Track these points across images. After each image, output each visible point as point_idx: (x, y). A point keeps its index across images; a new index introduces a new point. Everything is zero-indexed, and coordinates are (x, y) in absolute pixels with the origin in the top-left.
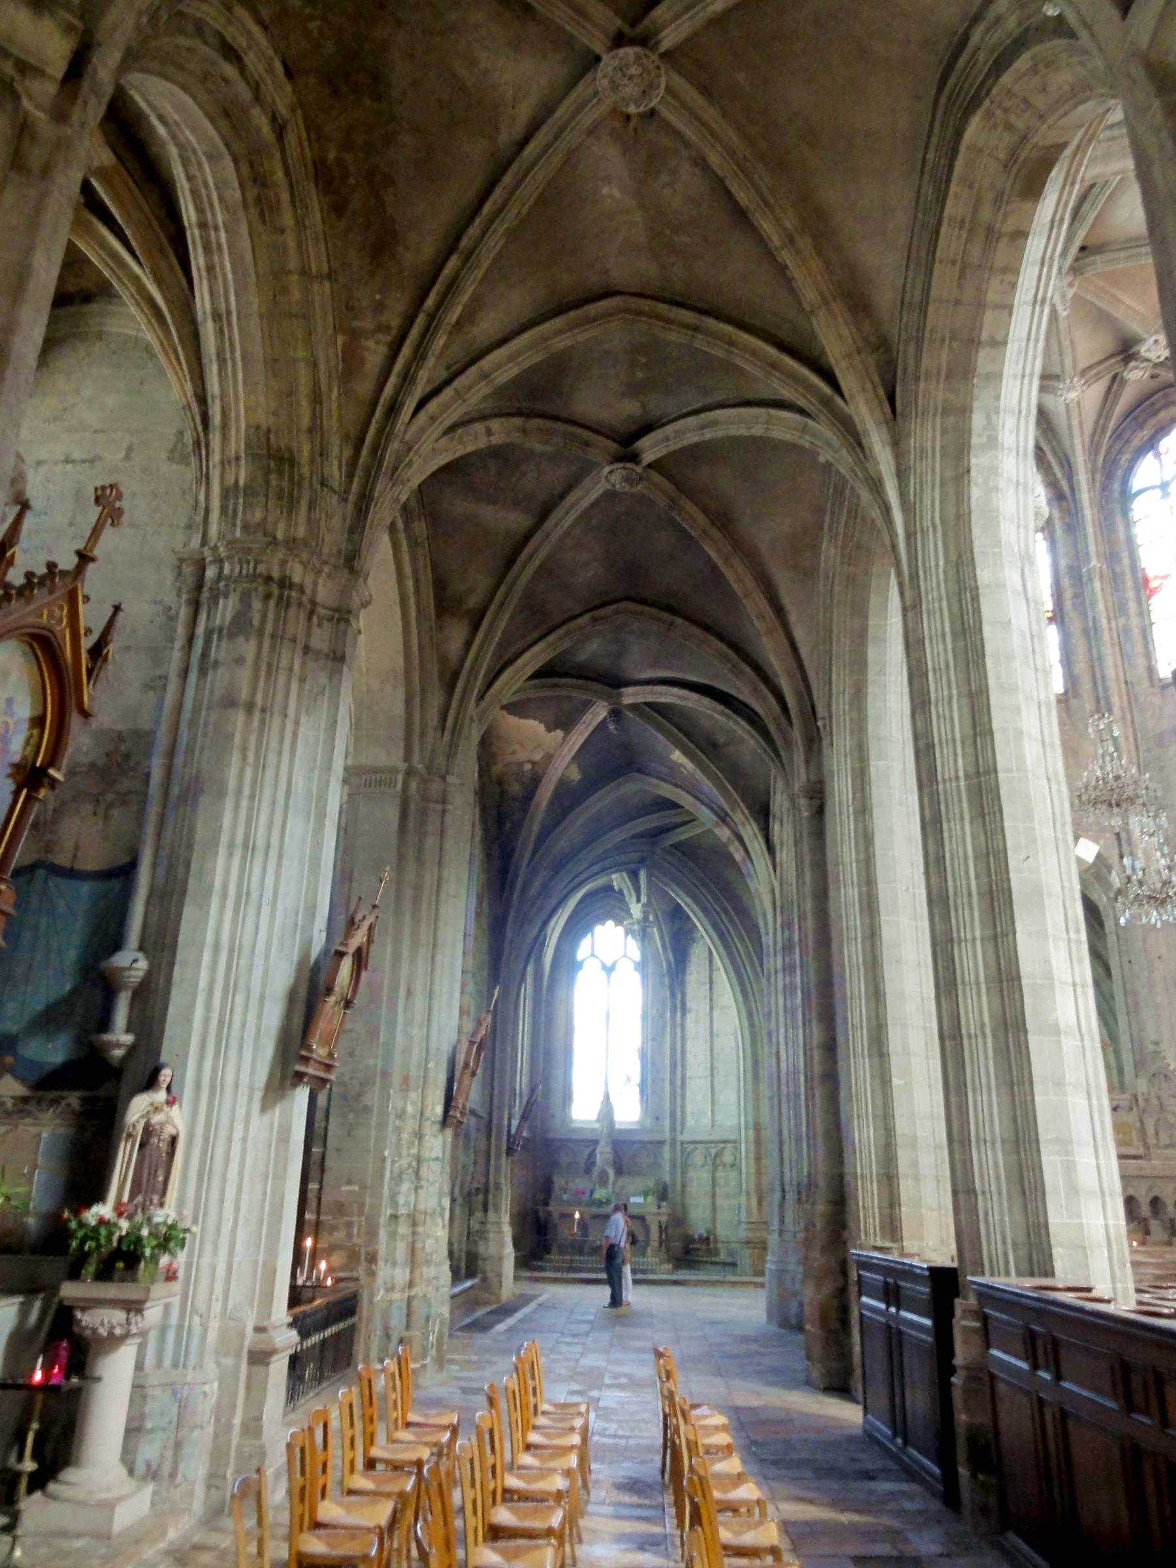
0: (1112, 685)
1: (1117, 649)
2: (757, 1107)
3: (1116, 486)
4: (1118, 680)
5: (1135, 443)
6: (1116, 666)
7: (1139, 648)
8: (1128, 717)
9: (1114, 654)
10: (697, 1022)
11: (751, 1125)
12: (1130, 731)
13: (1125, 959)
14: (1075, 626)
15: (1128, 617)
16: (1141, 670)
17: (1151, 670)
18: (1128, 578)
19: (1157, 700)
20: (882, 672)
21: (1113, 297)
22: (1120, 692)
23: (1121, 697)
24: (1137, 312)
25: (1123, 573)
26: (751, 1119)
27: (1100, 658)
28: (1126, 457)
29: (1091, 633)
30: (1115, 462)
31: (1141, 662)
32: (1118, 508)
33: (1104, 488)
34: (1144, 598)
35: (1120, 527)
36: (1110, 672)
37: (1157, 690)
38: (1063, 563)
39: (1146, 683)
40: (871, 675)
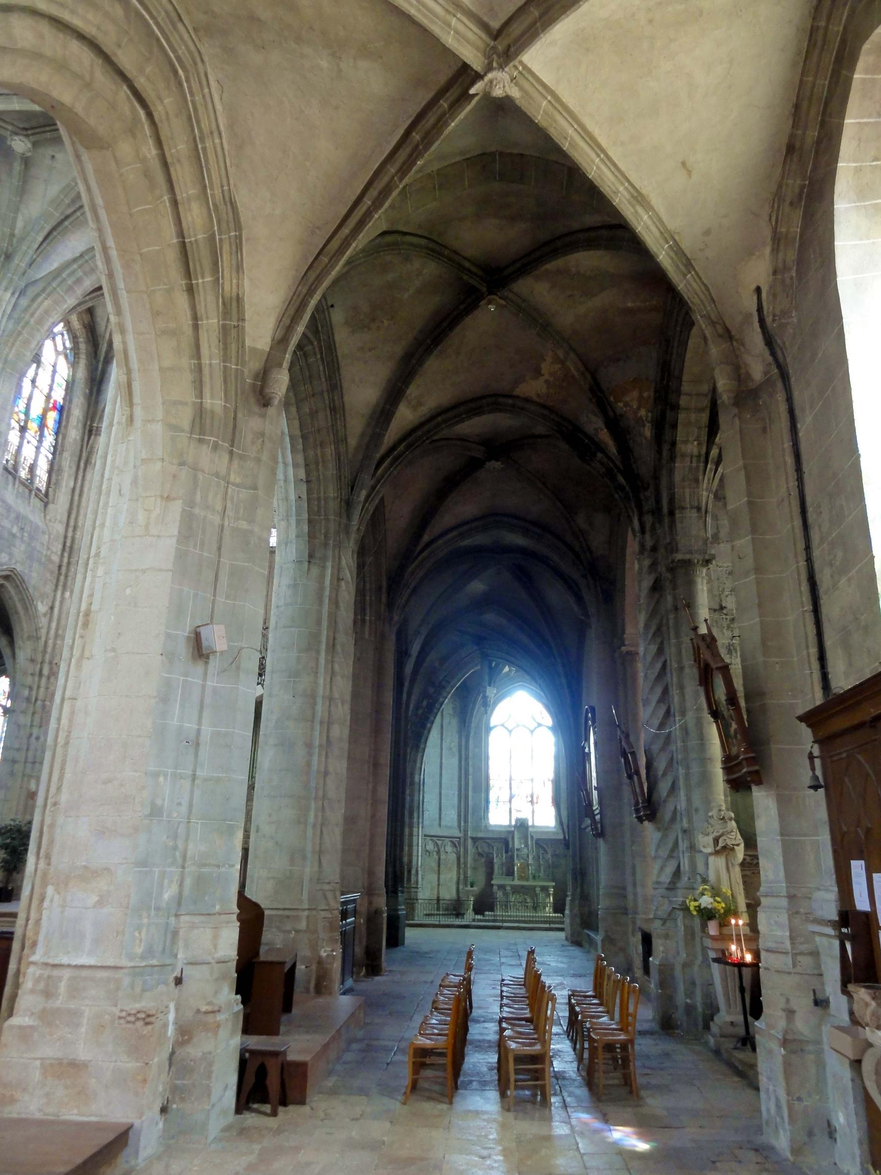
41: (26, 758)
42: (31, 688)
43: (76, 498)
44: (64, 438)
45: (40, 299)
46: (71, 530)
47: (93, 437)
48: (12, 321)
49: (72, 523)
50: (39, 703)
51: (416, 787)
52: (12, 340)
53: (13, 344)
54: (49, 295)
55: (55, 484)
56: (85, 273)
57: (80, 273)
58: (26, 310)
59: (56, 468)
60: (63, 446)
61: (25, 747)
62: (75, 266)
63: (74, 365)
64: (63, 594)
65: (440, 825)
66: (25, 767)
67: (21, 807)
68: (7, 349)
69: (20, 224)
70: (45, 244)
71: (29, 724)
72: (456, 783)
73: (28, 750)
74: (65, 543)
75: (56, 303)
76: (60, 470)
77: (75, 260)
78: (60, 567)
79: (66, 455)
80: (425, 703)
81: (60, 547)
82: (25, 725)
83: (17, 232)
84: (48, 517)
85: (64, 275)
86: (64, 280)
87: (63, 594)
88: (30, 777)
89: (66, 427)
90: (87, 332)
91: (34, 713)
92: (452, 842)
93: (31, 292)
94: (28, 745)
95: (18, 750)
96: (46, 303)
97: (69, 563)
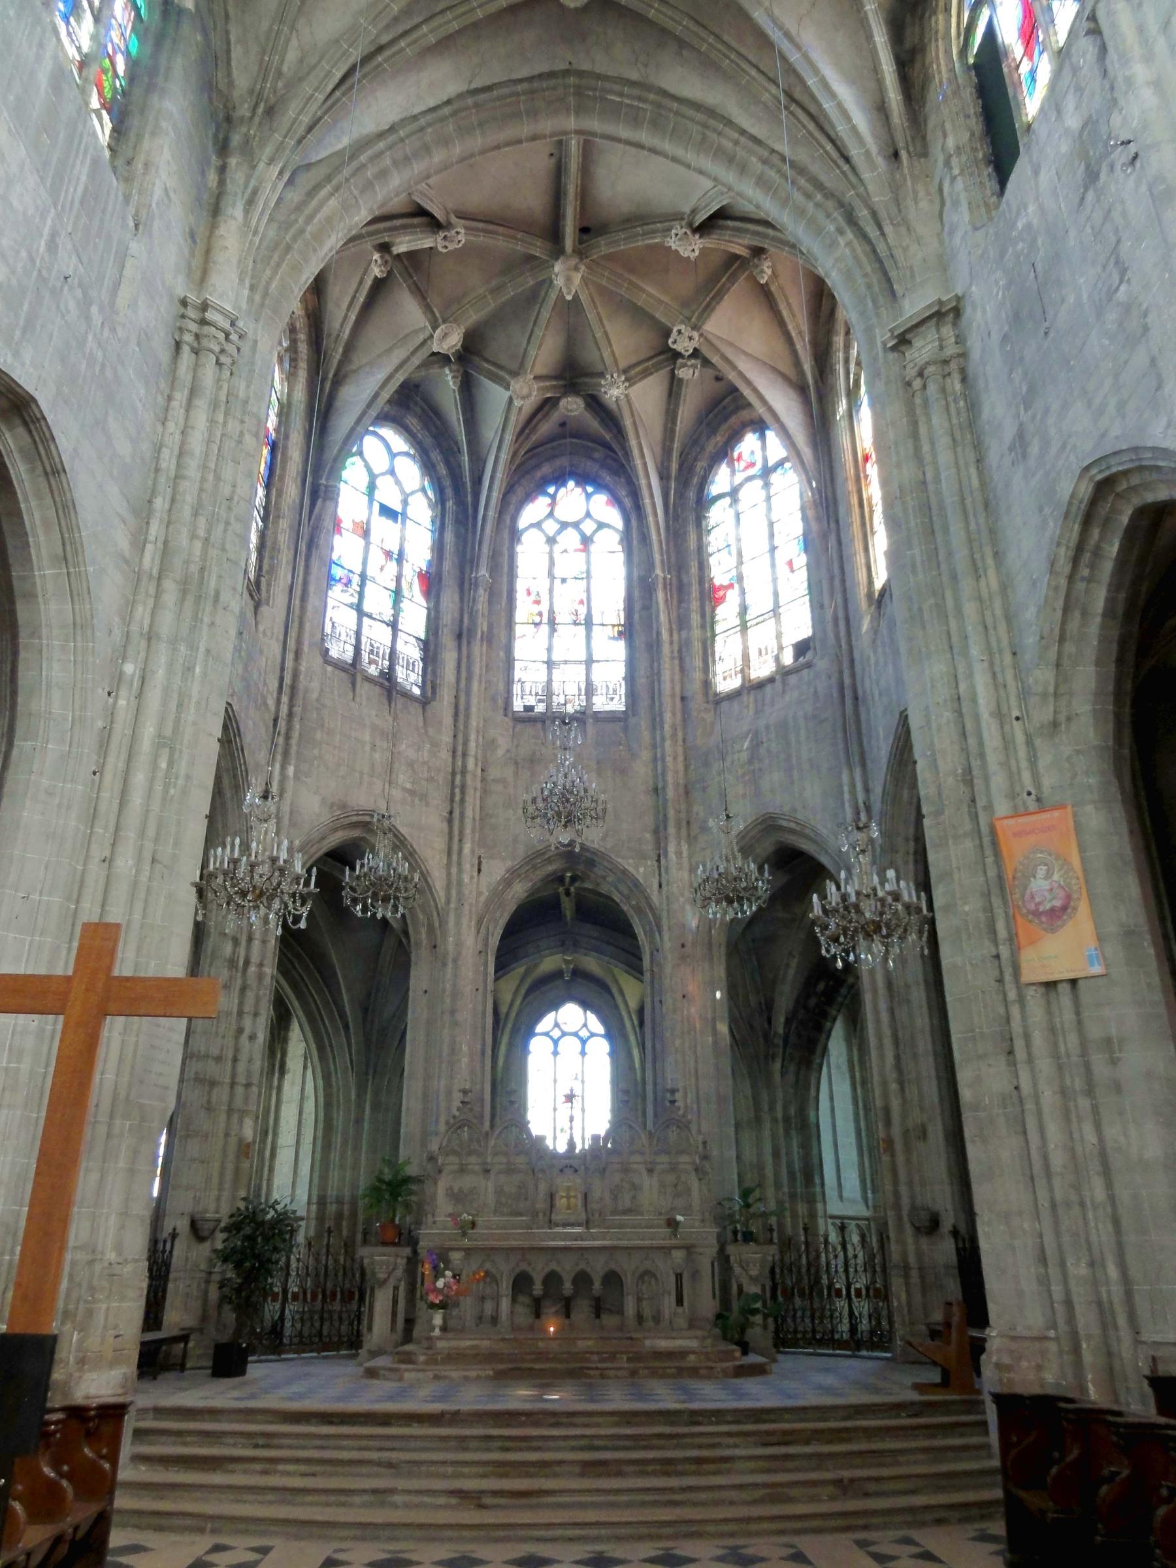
0: (667, 701)
1: (677, 662)
2: (324, 1178)
3: (692, 494)
4: (673, 696)
5: (710, 448)
6: (672, 681)
7: (698, 663)
8: (680, 734)
9: (672, 670)
10: (293, 1083)
11: (315, 1199)
12: (680, 750)
13: (657, 999)
14: (640, 640)
15: (690, 629)
16: (696, 686)
17: (707, 684)
18: (695, 589)
19: (709, 717)
20: (35, 633)
21: (631, 283)
22: (674, 706)
23: (674, 714)
24: (661, 302)
25: (690, 584)
26: (315, 1193)
27: (659, 672)
28: (701, 465)
29: (653, 647)
30: (691, 469)
31: (698, 676)
32: (692, 518)
33: (680, 495)
34: (708, 609)
35: (693, 536)
36: (667, 687)
37: (711, 706)
38: (636, 574)
39: (700, 698)
40: (23, 639)
41: (234, 1075)
42: (236, 941)
43: (297, 602)
44: (280, 494)
45: (324, 192)
46: (290, 656)
47: (319, 502)
48: (275, 225)
49: (291, 644)
50: (252, 969)
51: (814, 1130)
52: (276, 257)
53: (278, 265)
54: (337, 189)
55: (268, 572)
56: (395, 163)
57: (387, 161)
58: (299, 208)
59: (269, 544)
60: (278, 509)
61: (230, 1055)
62: (382, 145)
63: (290, 377)
64: (283, 768)
65: (841, 1197)
66: (232, 1095)
67: (229, 1176)
68: (268, 272)
69: (292, 55)
70: (338, 93)
71: (235, 1010)
72: (851, 1126)
73: (235, 1060)
74: (282, 679)
75: (346, 207)
76: (275, 549)
77: (381, 135)
78: (276, 720)
79: (284, 524)
80: (821, 986)
81: (276, 685)
82: (229, 1014)
83: (285, 69)
84: (261, 628)
85: (363, 158)
86: (363, 166)
87: (283, 768)
88: (243, 1113)
89: (282, 478)
90: (310, 326)
91: (243, 989)
92: (858, 1226)
93: (306, 181)
94: (237, 1050)
95: (218, 1059)
96: (333, 202)
97: (290, 715)
